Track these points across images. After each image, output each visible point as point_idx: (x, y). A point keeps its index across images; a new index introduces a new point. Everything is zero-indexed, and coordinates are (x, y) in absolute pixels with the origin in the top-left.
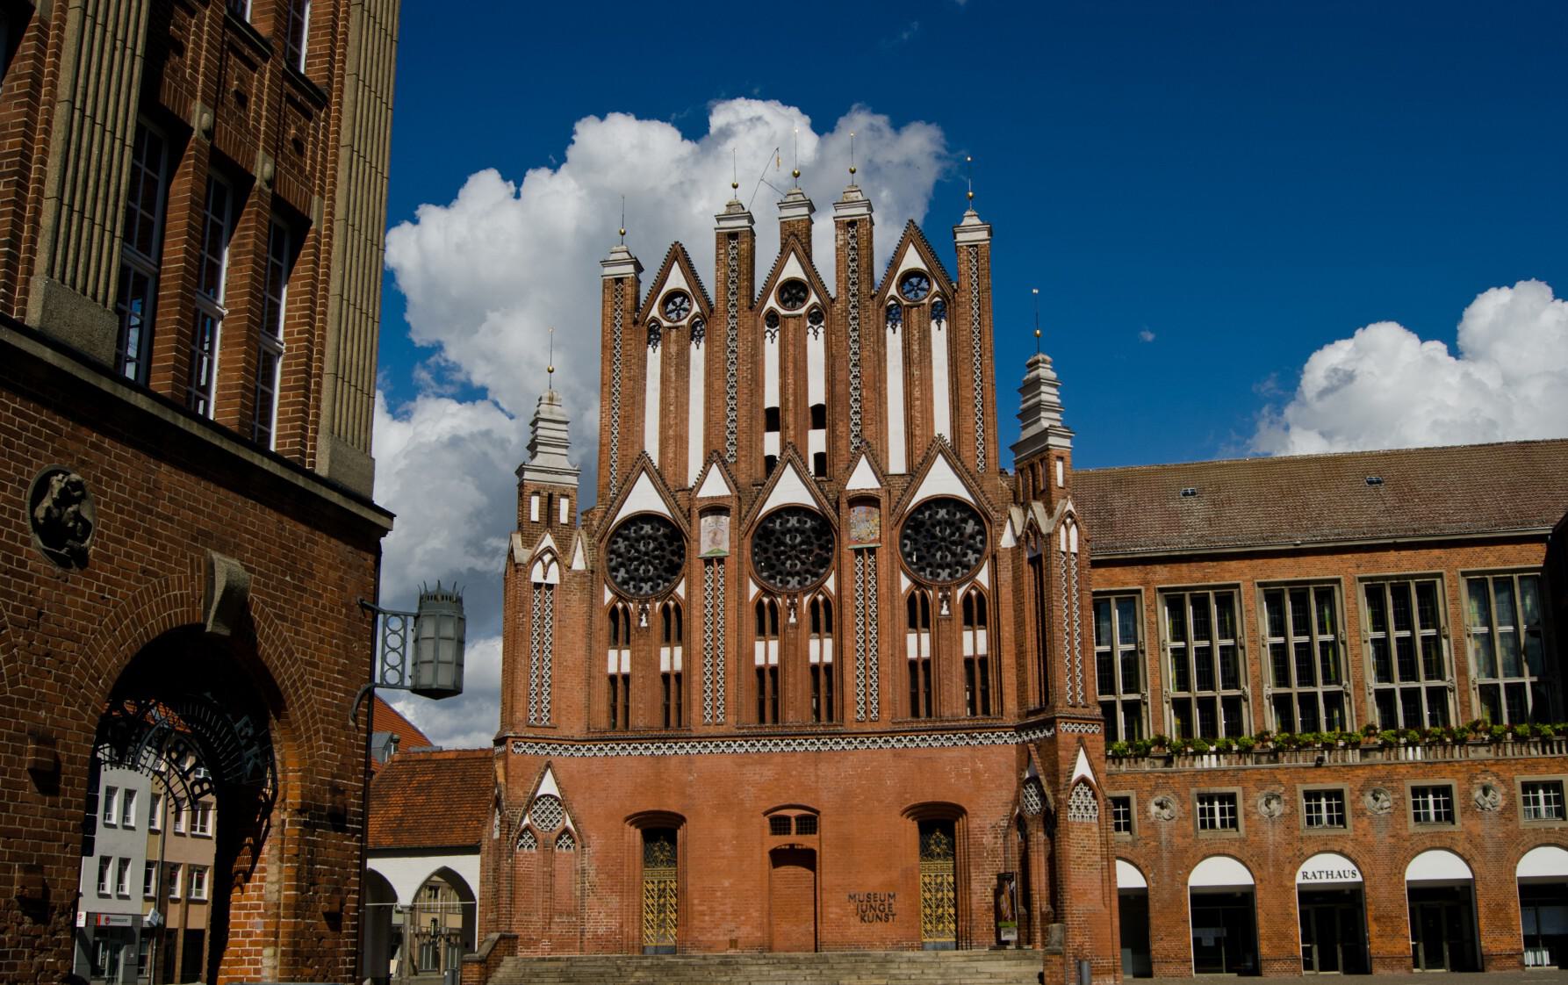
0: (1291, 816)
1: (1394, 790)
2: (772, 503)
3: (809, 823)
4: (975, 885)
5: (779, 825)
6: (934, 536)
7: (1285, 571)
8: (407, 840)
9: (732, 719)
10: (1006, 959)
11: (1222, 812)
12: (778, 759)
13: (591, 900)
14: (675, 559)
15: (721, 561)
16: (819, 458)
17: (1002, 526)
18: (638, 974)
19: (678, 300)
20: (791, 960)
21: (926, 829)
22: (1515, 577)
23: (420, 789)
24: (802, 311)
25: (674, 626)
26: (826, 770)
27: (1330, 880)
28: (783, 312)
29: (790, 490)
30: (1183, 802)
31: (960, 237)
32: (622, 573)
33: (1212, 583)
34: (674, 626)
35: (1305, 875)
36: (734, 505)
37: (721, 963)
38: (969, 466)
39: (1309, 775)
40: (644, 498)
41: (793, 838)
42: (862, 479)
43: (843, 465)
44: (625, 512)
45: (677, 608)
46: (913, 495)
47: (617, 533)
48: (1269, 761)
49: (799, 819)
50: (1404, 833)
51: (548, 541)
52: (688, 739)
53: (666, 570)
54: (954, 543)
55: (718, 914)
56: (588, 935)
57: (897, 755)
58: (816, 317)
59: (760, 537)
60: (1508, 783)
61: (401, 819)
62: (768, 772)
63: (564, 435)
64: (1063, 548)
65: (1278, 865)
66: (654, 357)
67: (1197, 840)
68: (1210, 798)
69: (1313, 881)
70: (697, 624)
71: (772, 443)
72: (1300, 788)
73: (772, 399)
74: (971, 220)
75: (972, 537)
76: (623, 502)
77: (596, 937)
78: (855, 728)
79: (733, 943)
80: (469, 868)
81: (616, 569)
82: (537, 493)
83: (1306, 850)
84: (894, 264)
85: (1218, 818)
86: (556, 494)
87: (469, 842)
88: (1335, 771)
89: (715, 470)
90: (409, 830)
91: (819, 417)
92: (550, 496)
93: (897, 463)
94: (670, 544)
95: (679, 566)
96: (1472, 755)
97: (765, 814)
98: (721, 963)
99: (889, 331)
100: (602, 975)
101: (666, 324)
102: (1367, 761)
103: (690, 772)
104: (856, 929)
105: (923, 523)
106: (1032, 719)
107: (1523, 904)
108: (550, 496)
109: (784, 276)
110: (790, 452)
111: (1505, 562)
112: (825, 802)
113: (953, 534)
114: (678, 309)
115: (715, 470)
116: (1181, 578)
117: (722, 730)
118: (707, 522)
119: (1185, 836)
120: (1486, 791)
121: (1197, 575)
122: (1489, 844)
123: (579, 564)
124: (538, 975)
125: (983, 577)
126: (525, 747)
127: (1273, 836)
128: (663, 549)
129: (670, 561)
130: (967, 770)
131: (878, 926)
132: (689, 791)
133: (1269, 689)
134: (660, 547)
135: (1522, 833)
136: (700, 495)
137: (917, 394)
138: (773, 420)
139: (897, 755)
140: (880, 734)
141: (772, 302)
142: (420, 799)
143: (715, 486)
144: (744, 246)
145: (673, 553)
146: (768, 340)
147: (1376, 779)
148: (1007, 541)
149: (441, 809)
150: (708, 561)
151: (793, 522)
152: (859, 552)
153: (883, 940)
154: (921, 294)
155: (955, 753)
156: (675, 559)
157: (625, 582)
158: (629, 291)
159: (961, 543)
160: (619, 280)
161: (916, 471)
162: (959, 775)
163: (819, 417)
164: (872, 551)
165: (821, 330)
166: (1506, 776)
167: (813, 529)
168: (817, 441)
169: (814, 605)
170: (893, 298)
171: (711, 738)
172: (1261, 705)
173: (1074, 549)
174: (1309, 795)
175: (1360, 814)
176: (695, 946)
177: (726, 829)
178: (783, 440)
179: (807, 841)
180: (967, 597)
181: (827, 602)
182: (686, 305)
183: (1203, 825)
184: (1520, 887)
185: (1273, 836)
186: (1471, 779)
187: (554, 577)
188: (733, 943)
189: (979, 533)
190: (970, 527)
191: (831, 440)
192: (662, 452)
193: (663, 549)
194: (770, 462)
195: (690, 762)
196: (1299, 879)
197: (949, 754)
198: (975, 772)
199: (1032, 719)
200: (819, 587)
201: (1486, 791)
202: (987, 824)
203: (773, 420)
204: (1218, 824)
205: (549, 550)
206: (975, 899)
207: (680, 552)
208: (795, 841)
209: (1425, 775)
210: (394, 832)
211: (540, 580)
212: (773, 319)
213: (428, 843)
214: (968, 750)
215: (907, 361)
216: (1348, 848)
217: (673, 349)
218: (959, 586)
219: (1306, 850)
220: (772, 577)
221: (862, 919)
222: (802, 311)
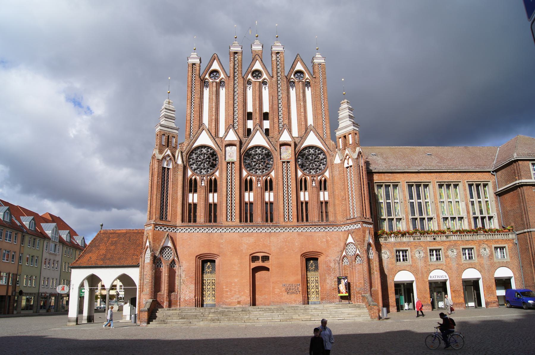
0: (426, 257)
1: (457, 249)
2: (252, 144)
3: (266, 258)
4: (328, 281)
5: (254, 259)
6: (308, 159)
7: (414, 178)
8: (108, 263)
10: (350, 307)
11: (403, 256)
12: (255, 235)
13: (183, 286)
14: (214, 162)
15: (233, 163)
16: (267, 131)
17: (333, 157)
18: (210, 315)
19: (215, 74)
20: (270, 309)
21: (308, 260)
22: (482, 183)
23: (112, 244)
24: (261, 80)
25: (213, 186)
26: (273, 239)
27: (439, 279)
28: (253, 80)
29: (258, 140)
30: (391, 253)
31: (315, 61)
32: (194, 166)
33: (392, 181)
34: (213, 186)
35: (431, 277)
36: (238, 144)
37: (242, 311)
39: (431, 244)
40: (204, 139)
41: (259, 263)
42: (285, 137)
43: (277, 133)
44: (196, 145)
45: (215, 179)
46: (302, 144)
47: (192, 152)
48: (418, 239)
49: (262, 257)
50: (461, 263)
51: (169, 152)
52: (221, 227)
53: (211, 166)
54: (315, 161)
55: (233, 292)
56: (182, 300)
57: (299, 234)
58: (264, 83)
59: (246, 156)
60: (490, 247)
61: (105, 255)
62: (252, 240)
63: (173, 115)
65: (422, 273)
66: (206, 92)
67: (396, 266)
68: (398, 251)
69: (433, 279)
70: (222, 185)
71: (250, 124)
72: (428, 248)
73: (250, 109)
74: (318, 56)
75: (322, 160)
76: (196, 140)
77: (185, 300)
78: (284, 224)
79: (239, 303)
80: (134, 274)
81: (191, 165)
82: (164, 135)
83: (431, 268)
84: (293, 67)
85: (401, 258)
86: (170, 136)
87: (134, 264)
88: (439, 243)
89: (231, 131)
90: (109, 259)
91: (266, 116)
92: (168, 136)
93: (295, 133)
94: (212, 157)
95: (216, 165)
96: (479, 238)
97: (250, 255)
98: (242, 311)
99: (291, 89)
100: (196, 316)
101: (211, 81)
102: (448, 240)
103: (222, 239)
104: (285, 297)
105: (304, 154)
106: (349, 222)
107: (496, 286)
108: (168, 136)
109: (254, 68)
110: (258, 127)
111: (479, 179)
112: (272, 250)
113: (315, 158)
114: (215, 76)
115: (231, 131)
116: (382, 179)
117: (234, 224)
118: (228, 148)
120: (485, 249)
121: (387, 178)
122: (486, 267)
123: (180, 162)
124: (169, 316)
125: (327, 174)
126: (159, 228)
127: (420, 264)
128: (210, 159)
129: (212, 163)
130: (324, 240)
131: (293, 296)
132: (222, 246)
133: (410, 217)
134: (209, 158)
135: (495, 263)
136: (226, 139)
137: (302, 110)
138: (250, 116)
139: (299, 234)
140: (293, 227)
141: (250, 77)
142: (113, 247)
143: (232, 137)
144: (240, 57)
145: (213, 160)
146: (248, 89)
147: (451, 245)
148: (337, 160)
149: (121, 251)
150: (228, 163)
151: (259, 151)
152: (283, 162)
153: (295, 301)
154: (301, 79)
155: (320, 234)
156: (214, 162)
157: (195, 170)
158: (198, 68)
159: (318, 161)
160: (195, 64)
161: (303, 138)
162: (322, 242)
163: (266, 116)
164: (288, 162)
165: (267, 87)
166: (490, 245)
167: (266, 154)
168: (266, 124)
169: (266, 180)
170: (292, 79)
171: (230, 226)
172: (408, 221)
174: (430, 250)
175: (447, 257)
176: (223, 304)
177: (236, 261)
178: (254, 123)
179: (265, 264)
180: (321, 181)
181: (271, 180)
182: (218, 75)
183: (397, 261)
184: (495, 280)
185: (420, 264)
186: (479, 246)
187: (171, 167)
188: (239, 303)
189: (324, 158)
190: (321, 156)
191: (272, 124)
192: (210, 124)
193: (210, 159)
194: (249, 130)
195: (222, 235)
196: (429, 279)
197: (318, 234)
198: (327, 241)
199: (349, 222)
200: (268, 175)
201: (485, 249)
202: (333, 258)
203: (250, 116)
204: (402, 260)
205: (168, 156)
206: (328, 285)
207: (215, 160)
208: (259, 265)
209: (466, 244)
210: (103, 260)
211: (165, 166)
212: (249, 82)
213: (118, 264)
214: (324, 233)
215: (298, 100)
216: (444, 268)
217: (214, 89)
218: (318, 176)
219: (431, 268)
220: (250, 170)
221: (288, 293)
222: (261, 80)
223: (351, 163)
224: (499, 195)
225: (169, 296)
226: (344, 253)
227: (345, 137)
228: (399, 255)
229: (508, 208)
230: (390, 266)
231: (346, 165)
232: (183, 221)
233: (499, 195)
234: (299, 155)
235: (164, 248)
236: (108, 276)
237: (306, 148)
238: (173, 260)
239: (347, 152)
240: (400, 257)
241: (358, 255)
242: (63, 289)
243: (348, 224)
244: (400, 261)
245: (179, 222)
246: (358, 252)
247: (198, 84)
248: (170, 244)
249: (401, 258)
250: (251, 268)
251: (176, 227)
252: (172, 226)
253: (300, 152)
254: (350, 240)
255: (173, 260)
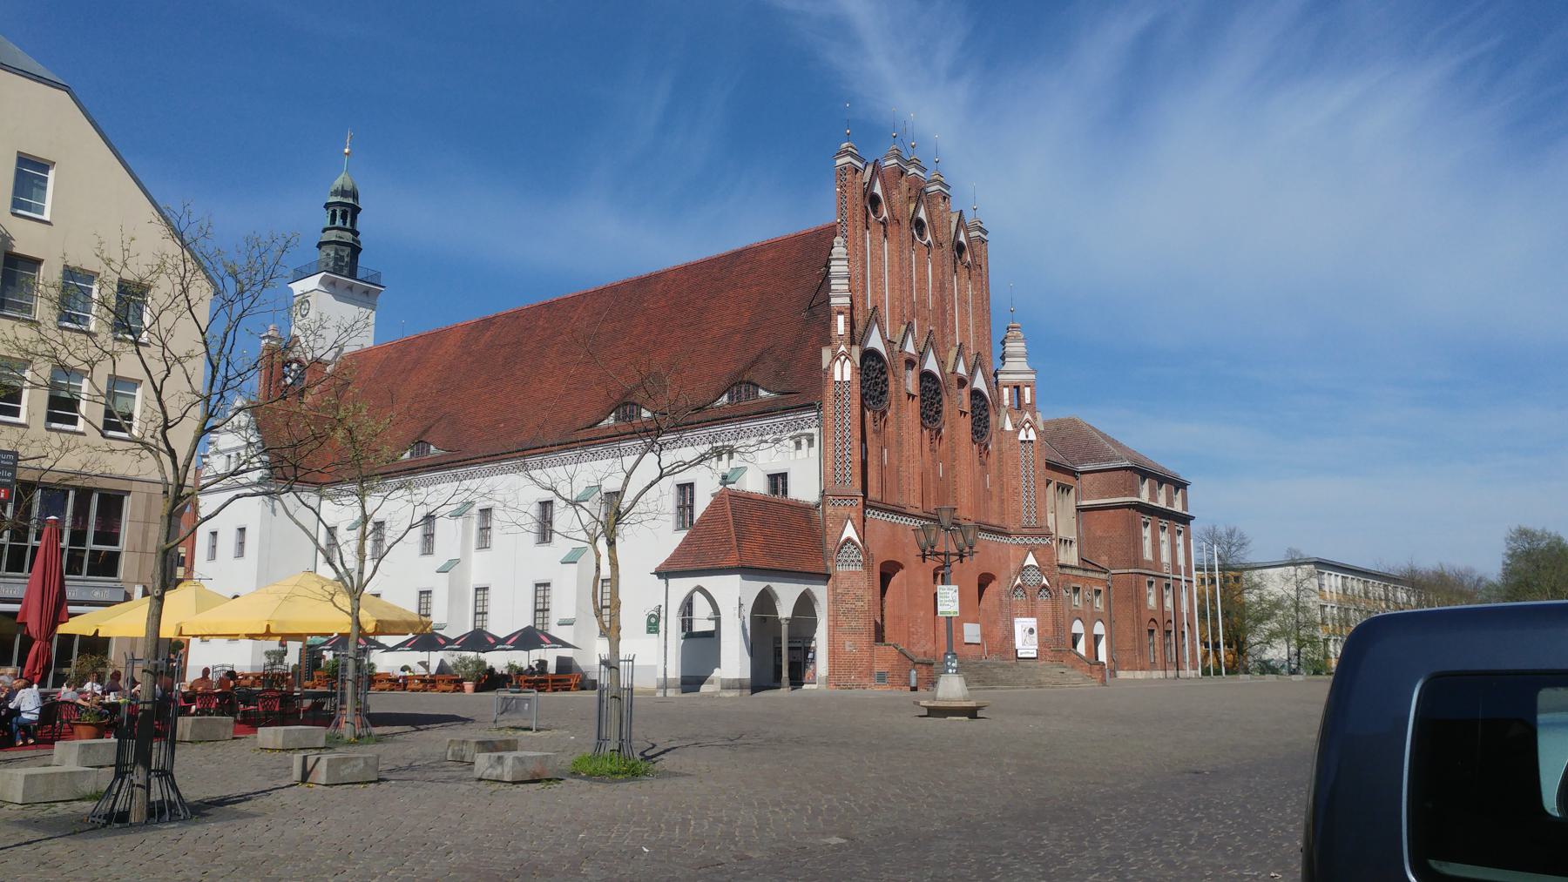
40: (875, 342)
223: (1032, 436)
224: (1080, 510)
226: (1018, 581)
227: (1017, 387)
229: (1099, 533)
231: (1022, 436)
233: (1080, 510)
236: (787, 595)
239: (1027, 416)
241: (1044, 587)
243: (1025, 535)
246: (1045, 581)
254: (1031, 560)
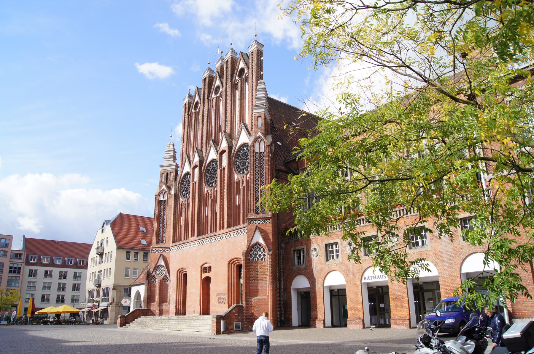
9: (196, 234)
13: (171, 297)
29: (213, 155)
35: (365, 279)
36: (198, 164)
38: (250, 129)
51: (164, 187)
64: (257, 151)
65: (354, 274)
86: (169, 173)
92: (167, 173)
108: (167, 173)
119: (322, 264)
123: (173, 192)
173: (262, 150)
187: (166, 199)
205: (164, 190)
225: (160, 305)
228: (333, 251)
230: (320, 266)
232: (173, 242)
234: (236, 158)
235: (156, 267)
237: (240, 147)
238: (166, 276)
240: (333, 253)
242: (126, 302)
244: (333, 258)
245: (171, 244)
247: (187, 119)
248: (162, 263)
249: (335, 254)
250: (202, 278)
251: (169, 247)
252: (166, 248)
253: (237, 154)
255: (166, 276)
